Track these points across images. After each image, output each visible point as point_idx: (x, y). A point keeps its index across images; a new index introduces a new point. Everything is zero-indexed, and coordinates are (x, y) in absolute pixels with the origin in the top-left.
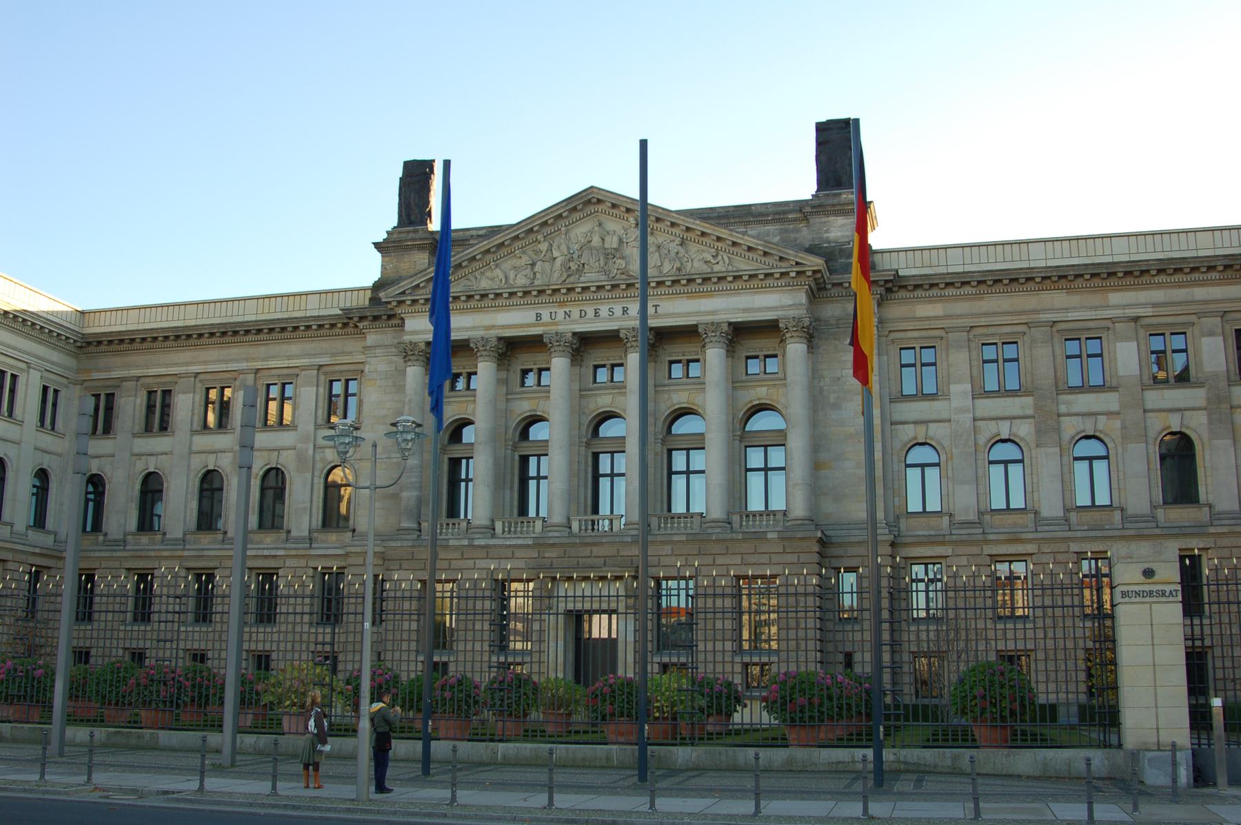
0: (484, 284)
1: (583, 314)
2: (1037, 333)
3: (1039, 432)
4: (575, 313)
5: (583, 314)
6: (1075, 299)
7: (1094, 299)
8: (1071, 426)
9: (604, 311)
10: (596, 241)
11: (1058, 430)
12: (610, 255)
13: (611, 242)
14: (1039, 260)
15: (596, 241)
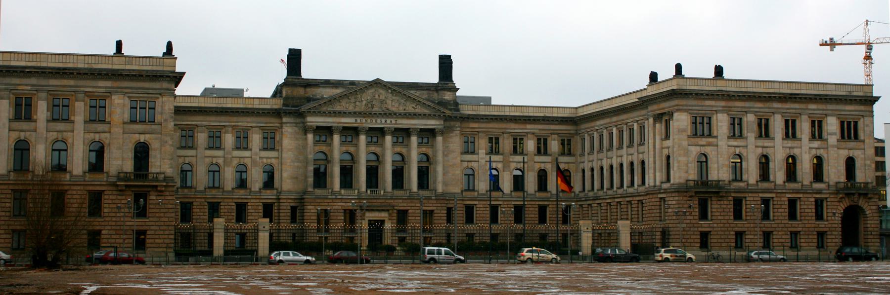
0: (338, 108)
1: (371, 121)
2: (505, 135)
3: (504, 167)
4: (369, 121)
5: (371, 121)
6: (517, 126)
7: (522, 126)
8: (513, 165)
9: (379, 121)
10: (377, 96)
11: (509, 166)
12: (382, 102)
13: (382, 97)
14: (508, 112)
15: (377, 96)
